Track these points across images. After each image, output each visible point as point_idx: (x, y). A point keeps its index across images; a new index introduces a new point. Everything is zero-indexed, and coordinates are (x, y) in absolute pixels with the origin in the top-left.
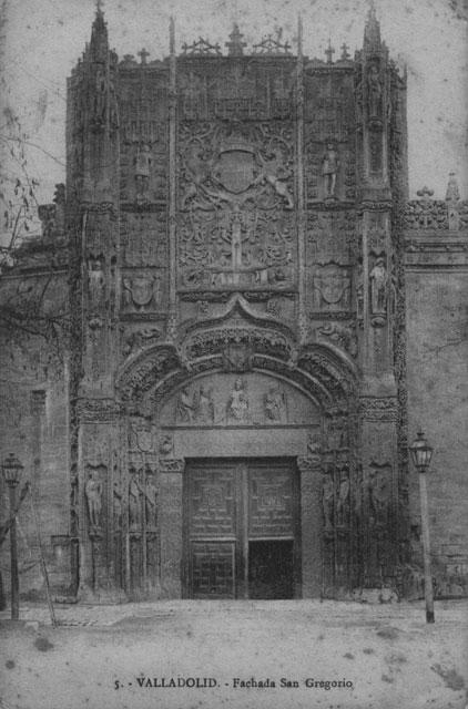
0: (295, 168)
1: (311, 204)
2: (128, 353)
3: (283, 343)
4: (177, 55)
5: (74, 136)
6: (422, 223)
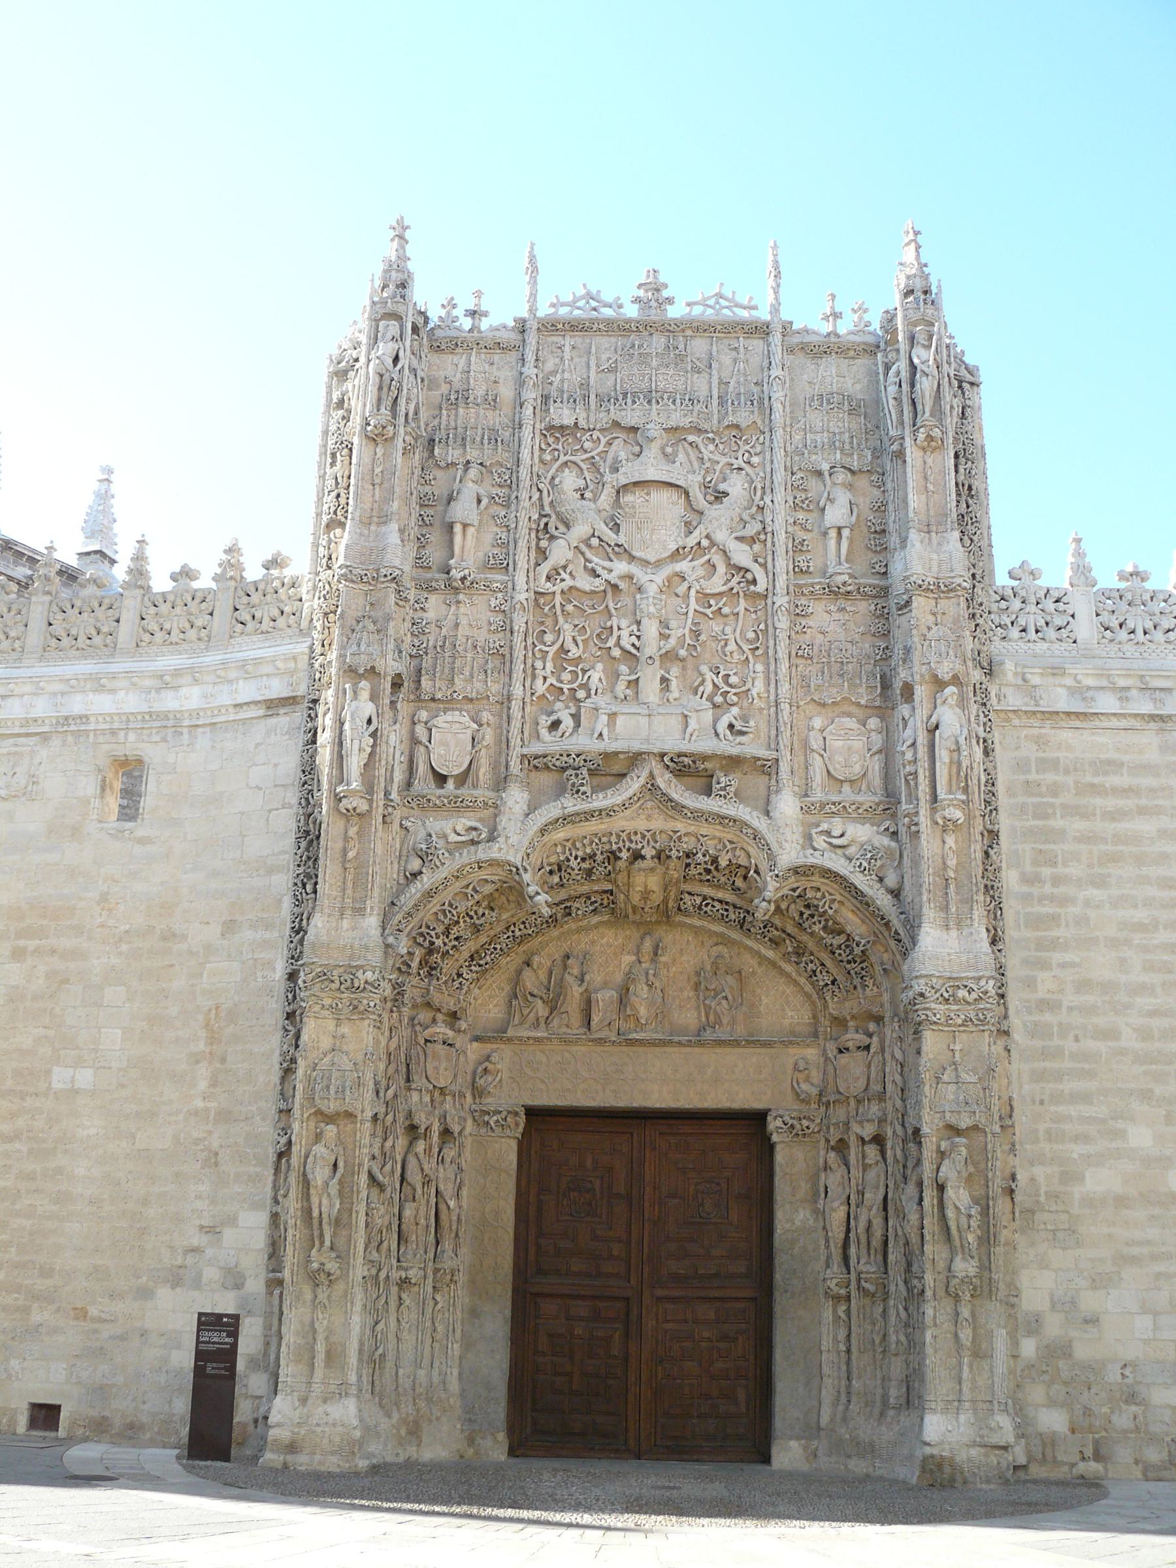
2: (416, 875)
3: (743, 861)
4: (540, 314)
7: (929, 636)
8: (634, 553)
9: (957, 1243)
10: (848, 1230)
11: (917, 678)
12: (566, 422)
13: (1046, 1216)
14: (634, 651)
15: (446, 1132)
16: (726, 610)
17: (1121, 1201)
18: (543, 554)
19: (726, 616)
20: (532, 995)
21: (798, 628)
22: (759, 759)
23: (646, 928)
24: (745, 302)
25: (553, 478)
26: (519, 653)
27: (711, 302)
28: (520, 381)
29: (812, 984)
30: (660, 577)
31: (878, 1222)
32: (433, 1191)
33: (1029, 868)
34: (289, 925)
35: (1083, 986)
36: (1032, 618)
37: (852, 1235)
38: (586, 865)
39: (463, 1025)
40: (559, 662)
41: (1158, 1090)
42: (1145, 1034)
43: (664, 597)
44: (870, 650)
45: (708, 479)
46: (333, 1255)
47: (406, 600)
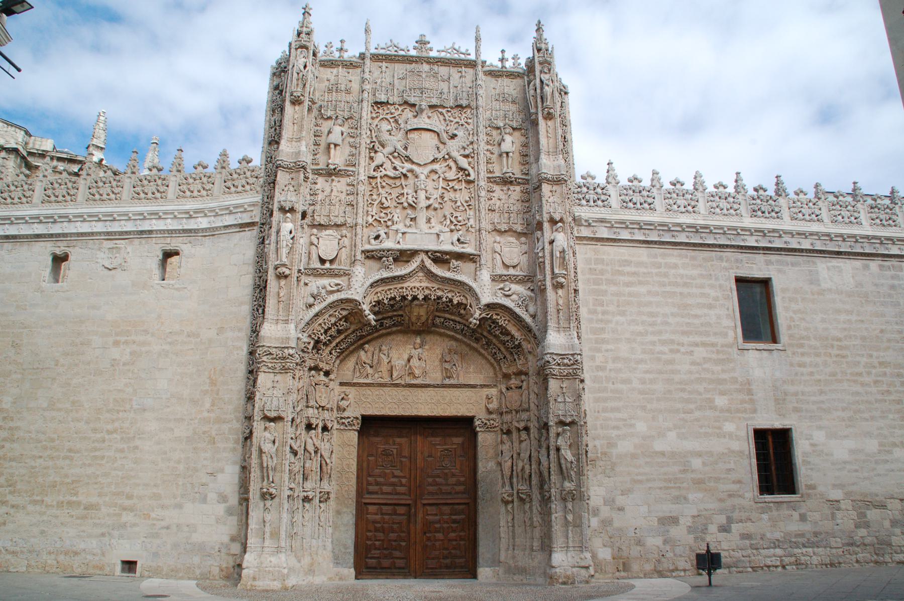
0: (475, 146)
1: (488, 178)
2: (311, 306)
3: (464, 301)
5: (273, 111)
6: (588, 201)
7: (549, 201)
8: (415, 161)
9: (566, 475)
10: (512, 471)
11: (545, 219)
12: (383, 100)
13: (601, 463)
14: (414, 205)
15: (325, 429)
16: (456, 187)
17: (634, 456)
18: (371, 158)
19: (456, 190)
20: (365, 363)
21: (489, 197)
22: (471, 255)
23: (418, 333)
24: (464, 51)
25: (377, 125)
26: (361, 205)
27: (449, 51)
28: (363, 81)
29: (494, 359)
30: (426, 170)
31: (527, 467)
32: (319, 455)
33: (591, 307)
34: (250, 329)
35: (616, 359)
36: (592, 196)
37: (515, 473)
38: (392, 303)
39: (332, 376)
40: (379, 209)
41: (649, 406)
42: (643, 381)
43: (427, 180)
44: (520, 208)
45: (448, 128)
46: (273, 485)
47: (308, 178)
